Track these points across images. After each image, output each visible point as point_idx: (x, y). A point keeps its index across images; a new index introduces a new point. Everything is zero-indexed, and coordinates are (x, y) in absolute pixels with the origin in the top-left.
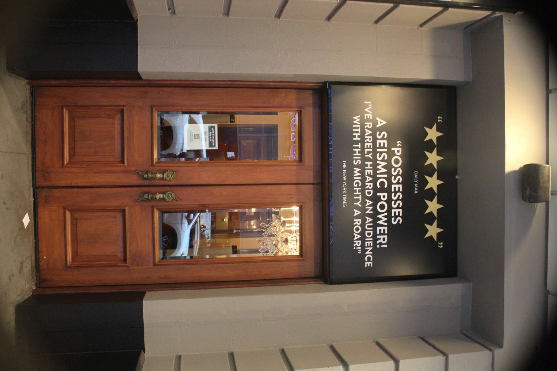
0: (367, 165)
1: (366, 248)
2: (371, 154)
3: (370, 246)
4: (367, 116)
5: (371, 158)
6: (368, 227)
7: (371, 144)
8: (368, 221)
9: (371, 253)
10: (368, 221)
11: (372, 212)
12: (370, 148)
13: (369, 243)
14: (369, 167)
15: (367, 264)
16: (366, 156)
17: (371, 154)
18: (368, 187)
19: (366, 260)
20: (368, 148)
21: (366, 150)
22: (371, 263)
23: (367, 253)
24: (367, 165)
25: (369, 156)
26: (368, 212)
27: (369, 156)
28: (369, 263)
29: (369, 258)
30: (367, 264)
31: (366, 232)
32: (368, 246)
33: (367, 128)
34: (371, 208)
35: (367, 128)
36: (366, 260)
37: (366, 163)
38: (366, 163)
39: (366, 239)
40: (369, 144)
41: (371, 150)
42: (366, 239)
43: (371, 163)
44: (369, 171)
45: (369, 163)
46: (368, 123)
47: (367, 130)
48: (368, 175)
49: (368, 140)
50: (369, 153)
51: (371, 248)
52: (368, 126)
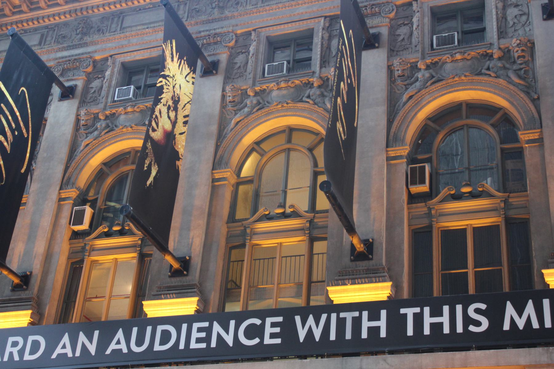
3: (208, 331)
6: (139, 343)
9: (232, 323)
10: (123, 347)
13: (195, 335)
18: (15, 350)
19: (257, 340)
23: (229, 339)
26: (92, 349)
28: (268, 330)
29: (251, 332)
30: (273, 336)
31: (157, 347)
32: (208, 340)
39: (182, 346)
42: (182, 346)
51: (217, 328)
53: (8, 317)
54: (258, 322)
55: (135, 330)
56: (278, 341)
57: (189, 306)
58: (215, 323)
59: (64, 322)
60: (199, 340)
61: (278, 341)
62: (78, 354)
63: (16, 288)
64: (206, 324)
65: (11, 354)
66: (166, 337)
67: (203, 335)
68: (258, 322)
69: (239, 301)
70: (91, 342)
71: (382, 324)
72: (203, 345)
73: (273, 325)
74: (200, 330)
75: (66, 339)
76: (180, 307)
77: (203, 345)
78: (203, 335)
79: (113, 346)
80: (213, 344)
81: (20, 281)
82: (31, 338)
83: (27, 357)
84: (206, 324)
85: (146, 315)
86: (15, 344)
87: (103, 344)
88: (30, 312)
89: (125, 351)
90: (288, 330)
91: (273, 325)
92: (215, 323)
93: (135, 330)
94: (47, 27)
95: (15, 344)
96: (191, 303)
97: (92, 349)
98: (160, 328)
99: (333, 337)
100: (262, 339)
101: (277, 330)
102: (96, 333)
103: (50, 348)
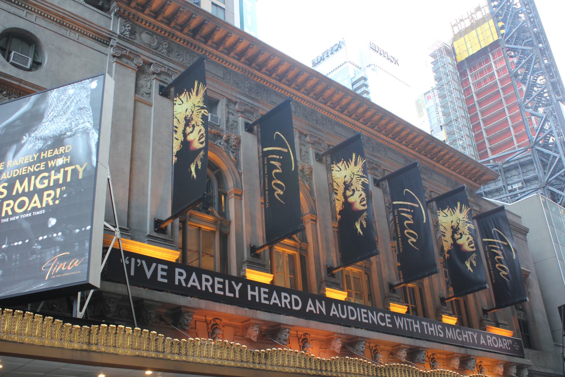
0: (253, 297)
1: (371, 322)
2: (233, 283)
3: (367, 313)
4: (162, 277)
5: (240, 284)
7: (217, 279)
8: (336, 313)
9: (375, 312)
10: (336, 313)
11: (323, 302)
12: (223, 284)
14: (256, 294)
16: (237, 296)
17: (233, 283)
19: (383, 324)
20: (223, 289)
21: (228, 294)
23: (375, 320)
24: (253, 297)
25: (237, 288)
26: (324, 310)
27: (237, 288)
28: (388, 320)
30: (389, 323)
33: (187, 280)
34: (318, 304)
35: (187, 280)
36: (383, 324)
37: (250, 299)
38: (250, 299)
40: (217, 286)
41: (227, 281)
42: (360, 320)
43: (249, 286)
44: (263, 296)
45: (250, 293)
46: (177, 277)
47: (191, 283)
48: (269, 299)
49: (209, 284)
50: (232, 290)
51: (370, 314)
52: (182, 278)
54: (383, 315)
62: (318, 313)
68: (383, 315)
71: (418, 326)
80: (371, 322)
89: (338, 316)
90: (393, 323)
94: (225, 68)
99: (407, 329)
100: (386, 323)
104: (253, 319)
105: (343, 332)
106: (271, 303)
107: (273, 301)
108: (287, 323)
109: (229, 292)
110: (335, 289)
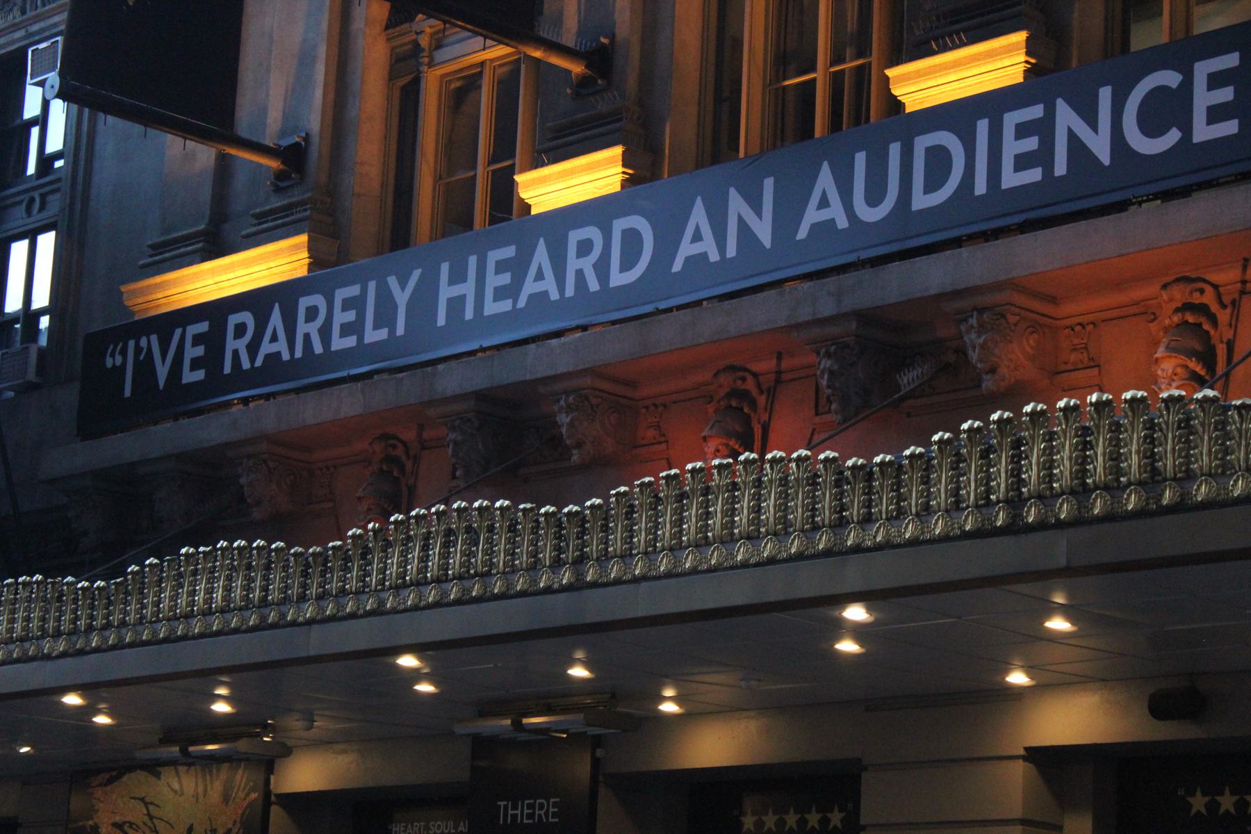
3: (1044, 128)
13: (1012, 147)
14: (467, 289)
15: (1216, 114)
18: (587, 264)
19: (1174, 136)
22: (1202, 70)
23: (1100, 145)
25: (402, 298)
26: (764, 231)
27: (402, 298)
30: (1216, 114)
31: (921, 201)
39: (980, 188)
42: (980, 188)
45: (446, 292)
53: (572, 172)
54: (1171, 78)
55: (860, 159)
56: (1230, 128)
57: (1007, 62)
58: (1060, 103)
59: (715, 160)
60: (1022, 163)
61: (1230, 128)
62: (731, 252)
63: (281, 182)
64: (1036, 112)
65: (580, 274)
66: (939, 161)
67: (1031, 144)
68: (1171, 78)
69: (1161, 14)
70: (759, 213)
72: (1034, 175)
73: (1215, 81)
74: (1023, 131)
75: (699, 216)
76: (983, 69)
77: (1034, 175)
78: (1031, 144)
79: (812, 216)
80: (1060, 168)
81: (283, 163)
82: (619, 225)
83: (618, 279)
84: (1036, 112)
85: (529, 207)
86: (585, 248)
87: (787, 215)
88: (618, 151)
89: (842, 223)
91: (1215, 81)
92: (1060, 103)
93: (860, 159)
95: (585, 248)
96: (1009, 50)
97: (764, 231)
98: (923, 143)
100: (1187, 129)
101: (1226, 94)
102: (769, 183)
103: (667, 244)
104: (430, 403)
105: (827, 308)
106: (522, 303)
107: (530, 287)
108: (550, 373)
109: (376, 327)
110: (944, 49)
